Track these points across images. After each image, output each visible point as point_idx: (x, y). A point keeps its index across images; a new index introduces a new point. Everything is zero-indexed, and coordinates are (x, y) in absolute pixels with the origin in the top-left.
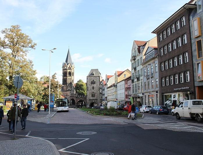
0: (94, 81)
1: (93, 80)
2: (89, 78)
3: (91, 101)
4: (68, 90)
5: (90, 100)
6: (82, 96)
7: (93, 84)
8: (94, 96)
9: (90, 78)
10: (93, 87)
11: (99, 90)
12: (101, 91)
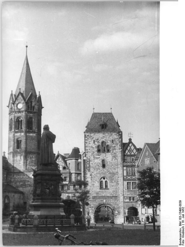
8: (106, 186)
10: (103, 161)
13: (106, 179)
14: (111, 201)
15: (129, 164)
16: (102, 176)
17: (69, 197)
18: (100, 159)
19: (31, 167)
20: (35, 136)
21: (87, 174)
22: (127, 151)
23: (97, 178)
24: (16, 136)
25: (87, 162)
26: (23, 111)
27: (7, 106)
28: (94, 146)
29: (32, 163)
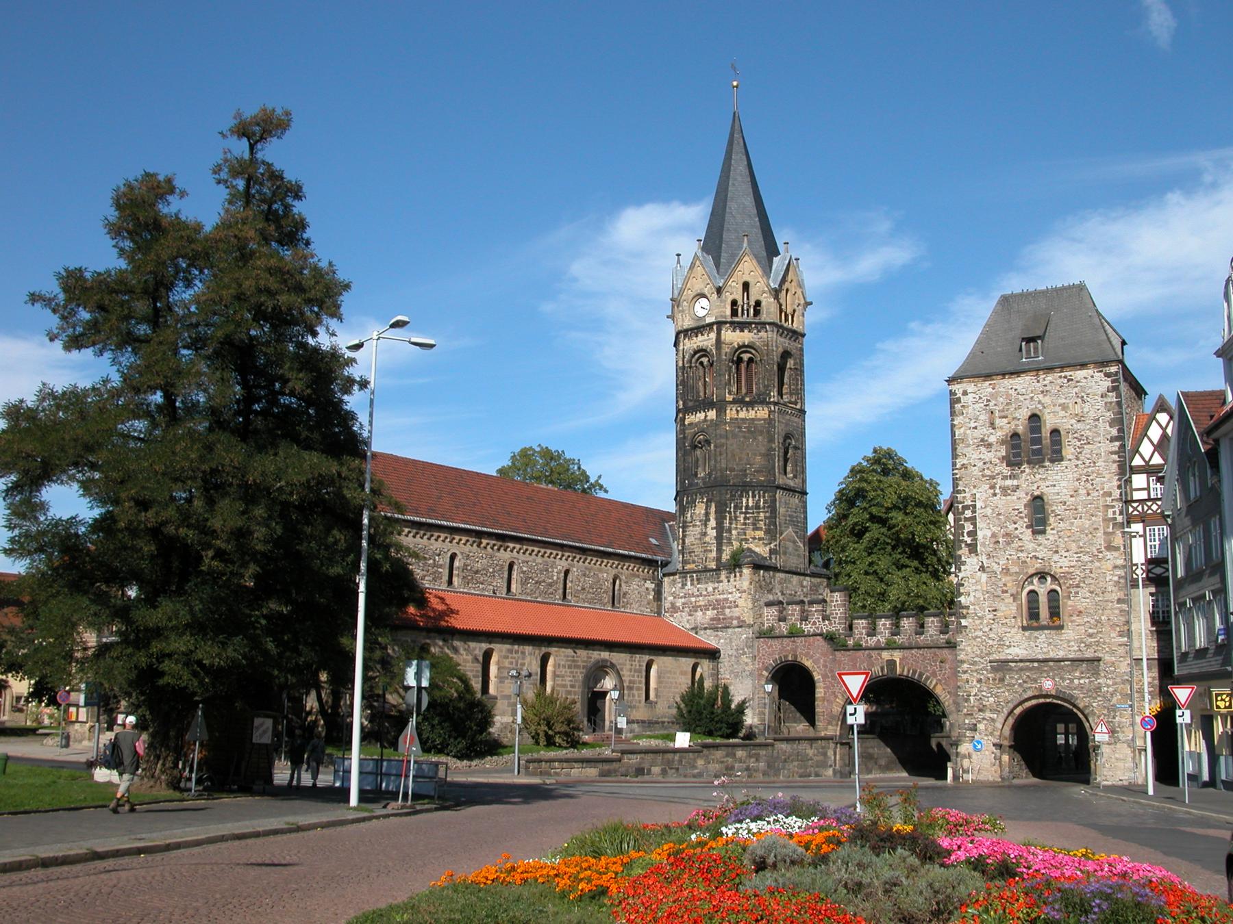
0: (1049, 422)
1: (1035, 418)
2: (973, 393)
3: (1014, 679)
4: (735, 564)
5: (1002, 666)
6: (896, 627)
7: (1037, 459)
8: (1055, 612)
9: (986, 387)
11: (1118, 540)
12: (1138, 544)
13: (1049, 579)
14: (1076, 681)
15: (1154, 507)
16: (1031, 571)
17: (892, 663)
18: (1018, 494)
19: (752, 546)
20: (764, 420)
21: (964, 563)
22: (1146, 448)
23: (1008, 578)
24: (690, 424)
25: (966, 508)
26: (711, 325)
27: (668, 317)
28: (992, 439)
29: (756, 529)
